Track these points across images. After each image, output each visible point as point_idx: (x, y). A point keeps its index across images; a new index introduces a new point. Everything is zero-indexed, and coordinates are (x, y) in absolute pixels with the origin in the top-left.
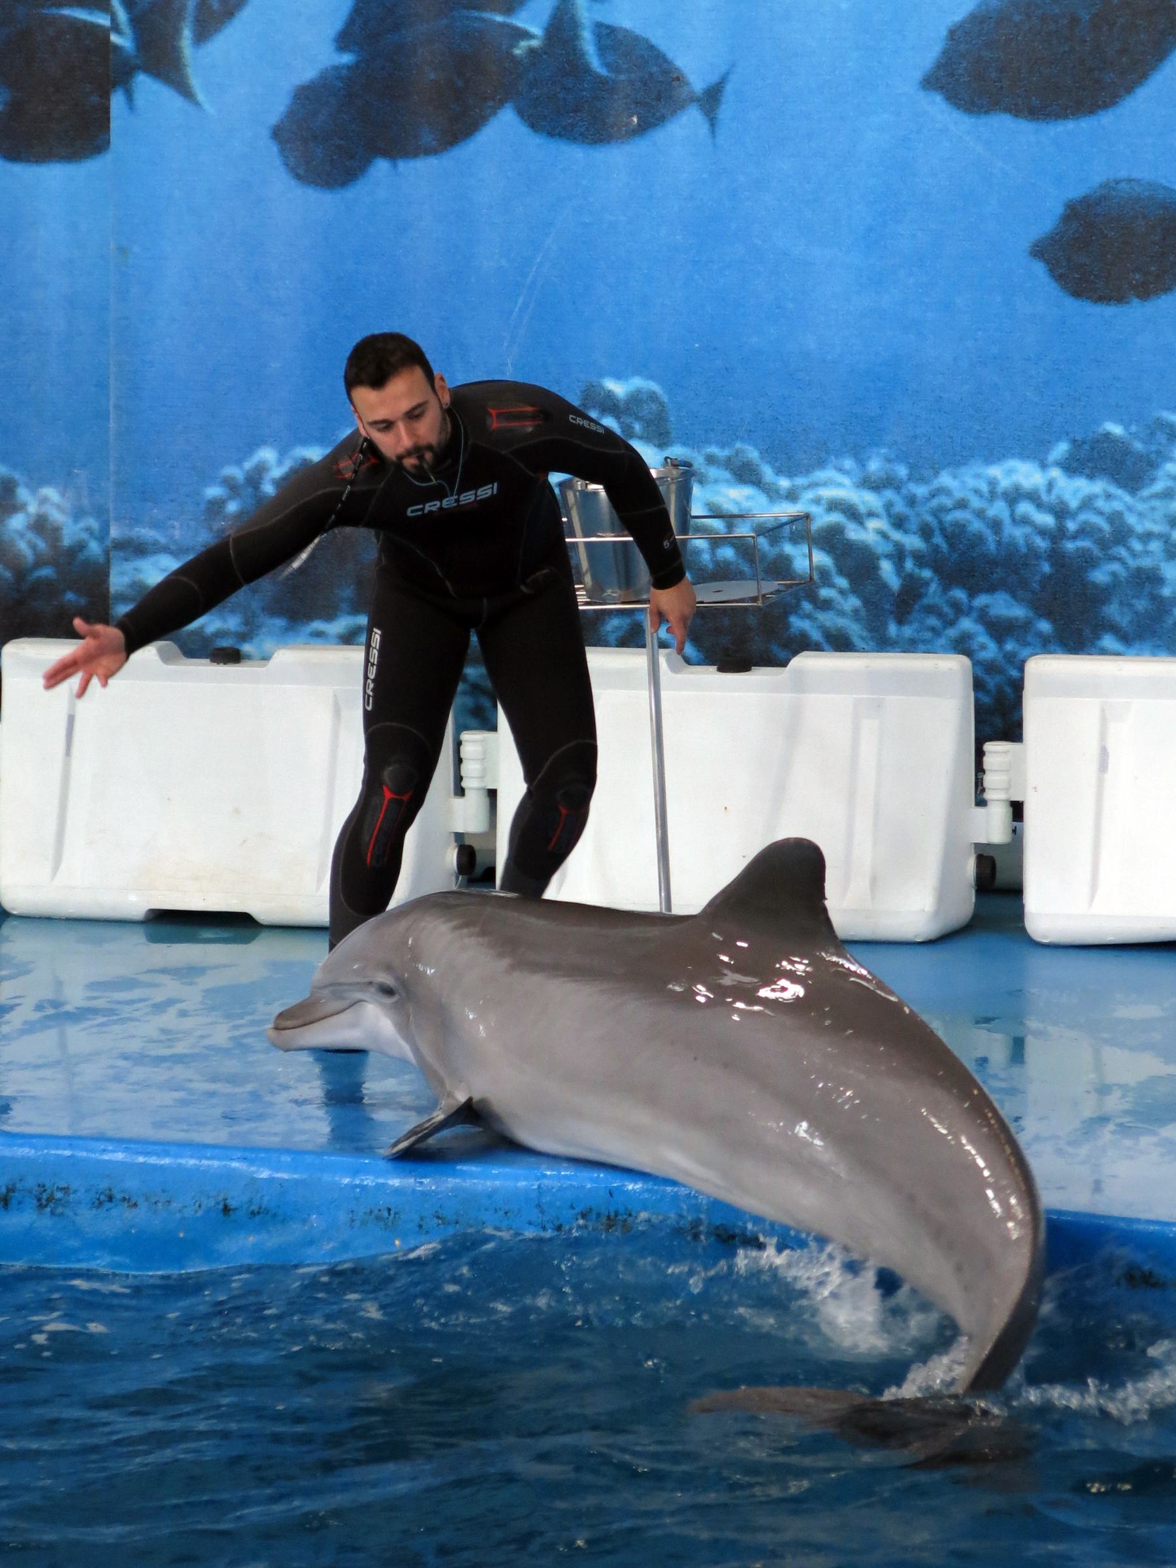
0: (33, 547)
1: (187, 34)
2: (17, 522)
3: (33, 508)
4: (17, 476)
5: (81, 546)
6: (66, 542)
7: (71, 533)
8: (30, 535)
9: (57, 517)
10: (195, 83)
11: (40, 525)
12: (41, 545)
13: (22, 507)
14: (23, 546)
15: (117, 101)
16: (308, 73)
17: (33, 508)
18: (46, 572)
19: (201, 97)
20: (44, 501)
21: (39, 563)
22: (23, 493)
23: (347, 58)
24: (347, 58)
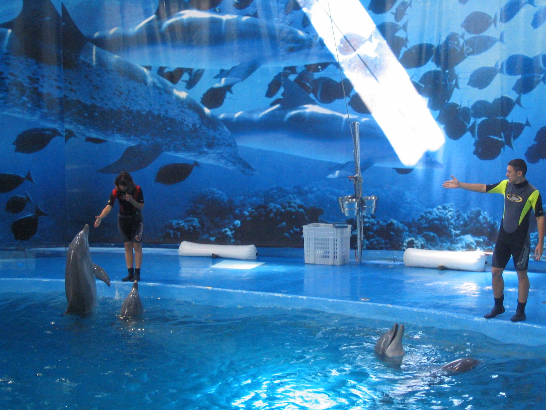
0: (484, 221)
1: (512, 139)
2: (481, 217)
3: (483, 215)
4: (481, 209)
5: (490, 221)
6: (488, 220)
7: (489, 219)
8: (483, 219)
9: (487, 216)
10: (513, 146)
11: (484, 218)
12: (485, 221)
13: (482, 215)
14: (482, 221)
15: (502, 149)
16: (530, 145)
17: (483, 215)
18: (485, 225)
19: (514, 148)
20: (485, 214)
21: (484, 223)
22: (482, 212)
23: (536, 143)
24: (536, 143)
